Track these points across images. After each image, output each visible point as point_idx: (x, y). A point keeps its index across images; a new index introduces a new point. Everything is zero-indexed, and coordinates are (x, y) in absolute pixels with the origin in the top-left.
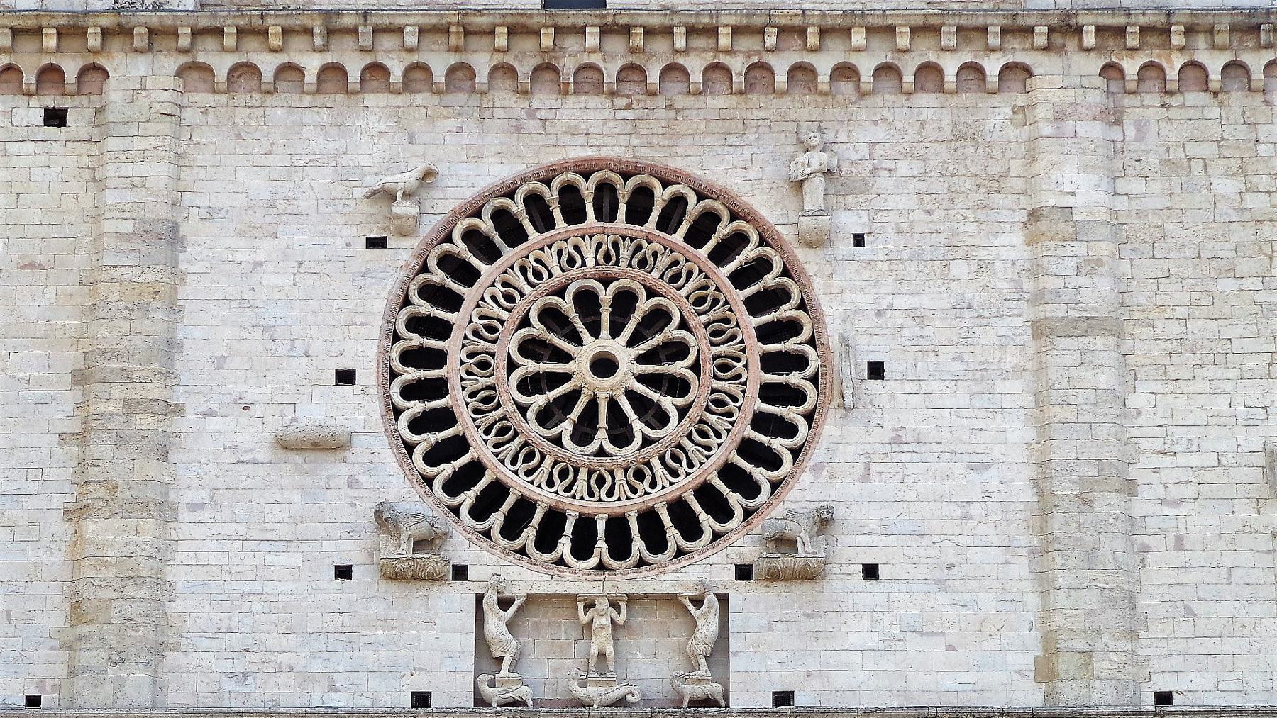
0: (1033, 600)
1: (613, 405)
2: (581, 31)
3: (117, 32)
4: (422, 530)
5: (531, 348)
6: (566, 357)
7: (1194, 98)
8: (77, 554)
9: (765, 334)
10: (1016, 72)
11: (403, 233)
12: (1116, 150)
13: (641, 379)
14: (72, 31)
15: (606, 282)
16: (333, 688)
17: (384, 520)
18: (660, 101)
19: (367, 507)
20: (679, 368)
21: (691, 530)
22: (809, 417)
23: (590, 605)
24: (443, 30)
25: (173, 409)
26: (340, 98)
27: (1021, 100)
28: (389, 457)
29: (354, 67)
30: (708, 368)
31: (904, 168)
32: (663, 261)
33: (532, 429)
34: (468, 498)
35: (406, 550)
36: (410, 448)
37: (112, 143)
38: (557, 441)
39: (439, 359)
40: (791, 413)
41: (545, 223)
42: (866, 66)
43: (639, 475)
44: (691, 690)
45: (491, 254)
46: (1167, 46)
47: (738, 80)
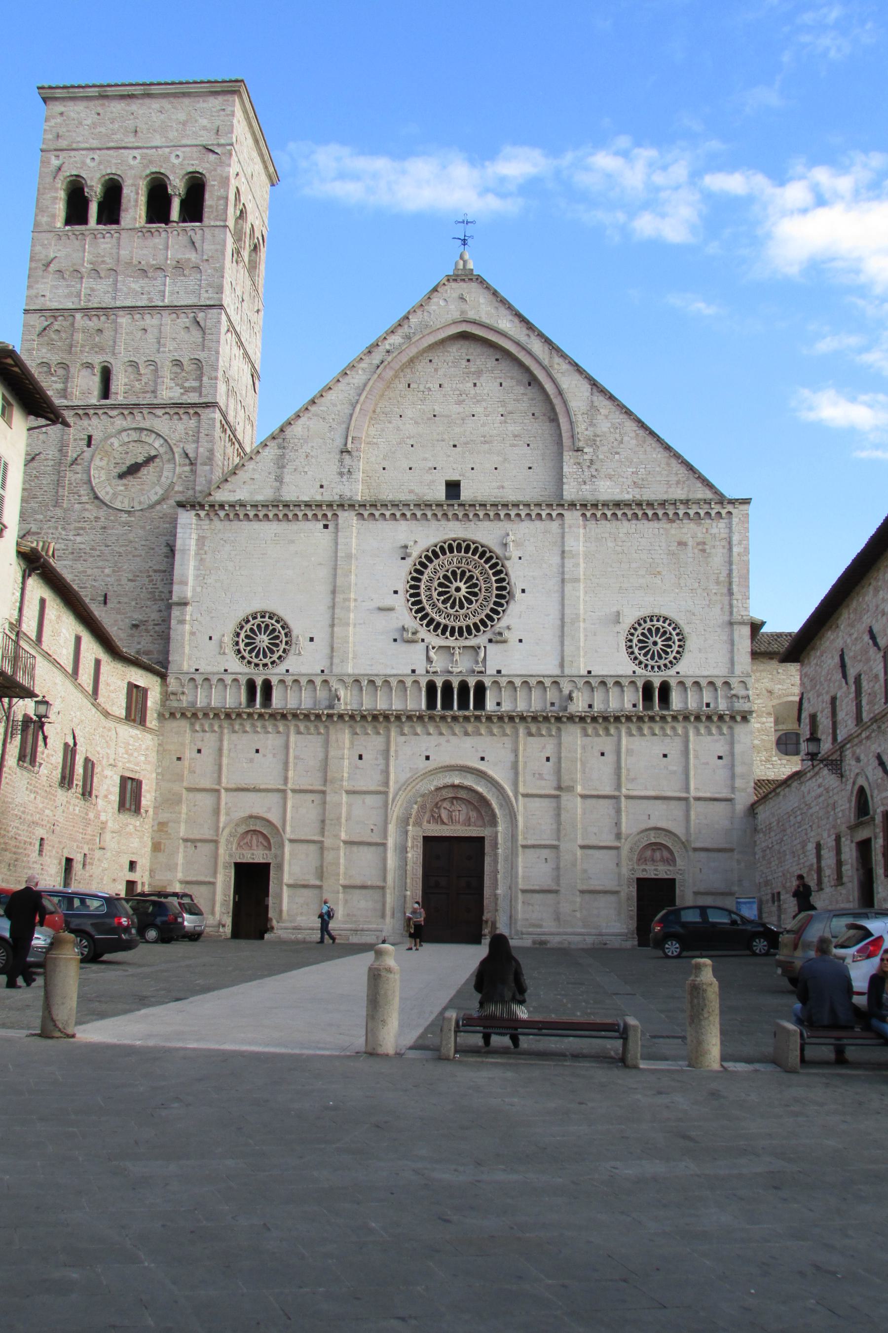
1: (460, 599)
2: (453, 505)
3: (341, 506)
4: (414, 630)
5: (441, 585)
6: (449, 587)
7: (604, 522)
9: (497, 581)
13: (467, 592)
14: (330, 505)
15: (459, 568)
16: (393, 668)
18: (472, 523)
19: (400, 625)
20: (476, 590)
21: (478, 630)
22: (507, 602)
23: (454, 648)
24: (419, 505)
27: (561, 522)
28: (406, 612)
29: (398, 514)
30: (483, 590)
31: (532, 540)
32: (473, 563)
33: (440, 605)
34: (425, 622)
35: (410, 635)
36: (411, 610)
38: (446, 608)
39: (418, 587)
40: (503, 601)
41: (444, 553)
42: (523, 514)
43: (466, 616)
44: (477, 669)
45: (431, 561)
46: (597, 509)
47: (492, 517)
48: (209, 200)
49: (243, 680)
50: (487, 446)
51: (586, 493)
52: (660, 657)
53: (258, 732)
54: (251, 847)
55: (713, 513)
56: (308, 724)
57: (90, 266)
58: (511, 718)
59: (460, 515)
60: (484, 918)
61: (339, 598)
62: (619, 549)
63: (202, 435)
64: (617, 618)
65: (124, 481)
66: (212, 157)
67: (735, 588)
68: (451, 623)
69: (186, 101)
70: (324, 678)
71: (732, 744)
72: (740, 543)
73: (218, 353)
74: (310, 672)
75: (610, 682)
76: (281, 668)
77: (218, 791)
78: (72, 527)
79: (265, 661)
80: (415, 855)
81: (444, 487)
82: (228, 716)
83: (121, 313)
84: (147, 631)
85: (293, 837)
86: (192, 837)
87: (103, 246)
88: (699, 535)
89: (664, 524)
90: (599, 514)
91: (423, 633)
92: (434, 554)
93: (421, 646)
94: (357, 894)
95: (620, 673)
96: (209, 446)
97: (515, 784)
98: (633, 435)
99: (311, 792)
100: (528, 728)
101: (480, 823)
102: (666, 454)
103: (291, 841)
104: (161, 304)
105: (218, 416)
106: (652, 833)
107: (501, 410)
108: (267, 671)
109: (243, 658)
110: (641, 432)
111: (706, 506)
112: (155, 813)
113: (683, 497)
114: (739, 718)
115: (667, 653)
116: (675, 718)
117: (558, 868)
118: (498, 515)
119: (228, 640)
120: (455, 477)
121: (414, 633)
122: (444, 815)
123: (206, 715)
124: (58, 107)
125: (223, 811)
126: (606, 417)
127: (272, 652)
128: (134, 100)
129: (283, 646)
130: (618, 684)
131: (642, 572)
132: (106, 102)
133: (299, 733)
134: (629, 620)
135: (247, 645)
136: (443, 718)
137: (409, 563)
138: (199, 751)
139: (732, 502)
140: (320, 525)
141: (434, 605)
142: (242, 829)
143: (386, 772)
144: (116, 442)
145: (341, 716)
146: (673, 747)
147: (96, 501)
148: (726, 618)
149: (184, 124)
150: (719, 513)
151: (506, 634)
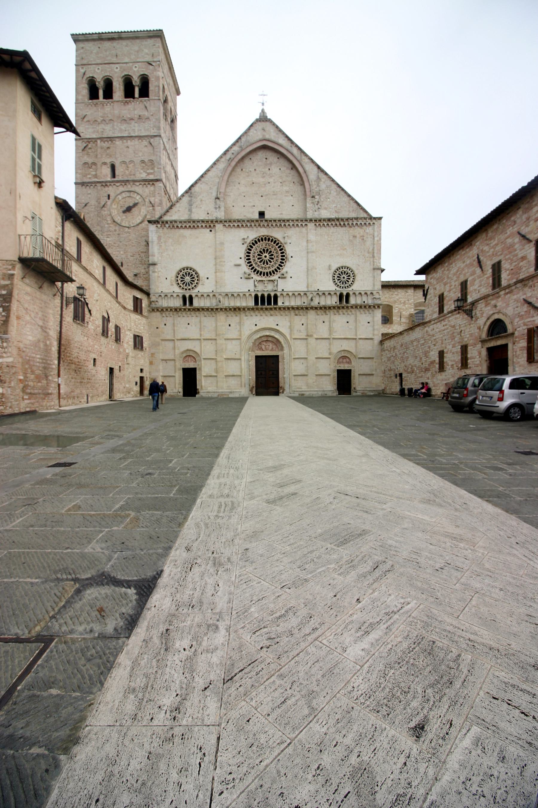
0: (306, 280)
3: (217, 221)
5: (259, 255)
7: (323, 228)
8: (216, 276)
10: (306, 225)
11: (246, 243)
12: (316, 233)
17: (245, 273)
19: (243, 272)
20: (273, 257)
21: (274, 273)
25: (224, 262)
26: (239, 229)
28: (245, 266)
29: (240, 225)
33: (259, 263)
37: (217, 234)
41: (259, 242)
42: (291, 224)
45: (254, 245)
48: (151, 87)
49: (181, 295)
50: (275, 197)
51: (316, 215)
52: (346, 283)
53: (188, 316)
54: (188, 362)
55: (367, 224)
56: (208, 312)
57: (102, 119)
58: (288, 308)
59: (266, 225)
60: (280, 386)
61: (218, 261)
62: (329, 239)
63: (156, 193)
64: (330, 267)
65: (125, 214)
66: (151, 67)
67: (375, 255)
68: (263, 271)
69: (138, 41)
70: (214, 294)
71: (373, 317)
72: (378, 236)
73: (160, 157)
74: (208, 291)
75: (327, 293)
76: (196, 290)
77: (174, 340)
78: (105, 234)
79: (189, 287)
80: (253, 363)
81: (258, 214)
82: (176, 310)
83: (117, 140)
84: (140, 277)
85: (204, 357)
86: (165, 359)
87: (107, 109)
88: (362, 233)
89: (347, 228)
90: (321, 224)
91: (253, 275)
92: (255, 242)
93: (252, 280)
94: (231, 379)
95: (331, 290)
96: (160, 198)
97: (291, 334)
98: (335, 190)
99: (211, 339)
100: (295, 312)
101: (277, 350)
102: (348, 198)
103: (204, 359)
104: (134, 135)
105: (161, 185)
106: (343, 352)
107: (280, 180)
108: (190, 292)
109: (180, 286)
110: (338, 189)
111: (365, 221)
112: (149, 350)
113: (355, 217)
114: (376, 307)
115: (348, 281)
116: (352, 307)
117: (307, 366)
118: (281, 225)
119: (174, 279)
120: (262, 210)
121: (249, 275)
122: (263, 347)
123: (167, 310)
124: (81, 45)
125: (176, 349)
126: (324, 182)
127: (192, 284)
128: (115, 41)
129: (196, 281)
130: (329, 294)
131: (339, 248)
132: (102, 42)
133: (205, 316)
134: (334, 268)
135: (181, 281)
136: (262, 309)
137: (245, 246)
138: (165, 325)
139: (375, 218)
140: (208, 230)
141: (256, 263)
142: (184, 355)
143: (240, 331)
144: (120, 197)
145: (221, 309)
146: (351, 318)
147: (115, 223)
148: (372, 267)
149: (138, 52)
150: (369, 224)
151: (285, 275)
